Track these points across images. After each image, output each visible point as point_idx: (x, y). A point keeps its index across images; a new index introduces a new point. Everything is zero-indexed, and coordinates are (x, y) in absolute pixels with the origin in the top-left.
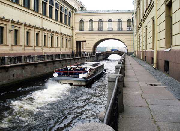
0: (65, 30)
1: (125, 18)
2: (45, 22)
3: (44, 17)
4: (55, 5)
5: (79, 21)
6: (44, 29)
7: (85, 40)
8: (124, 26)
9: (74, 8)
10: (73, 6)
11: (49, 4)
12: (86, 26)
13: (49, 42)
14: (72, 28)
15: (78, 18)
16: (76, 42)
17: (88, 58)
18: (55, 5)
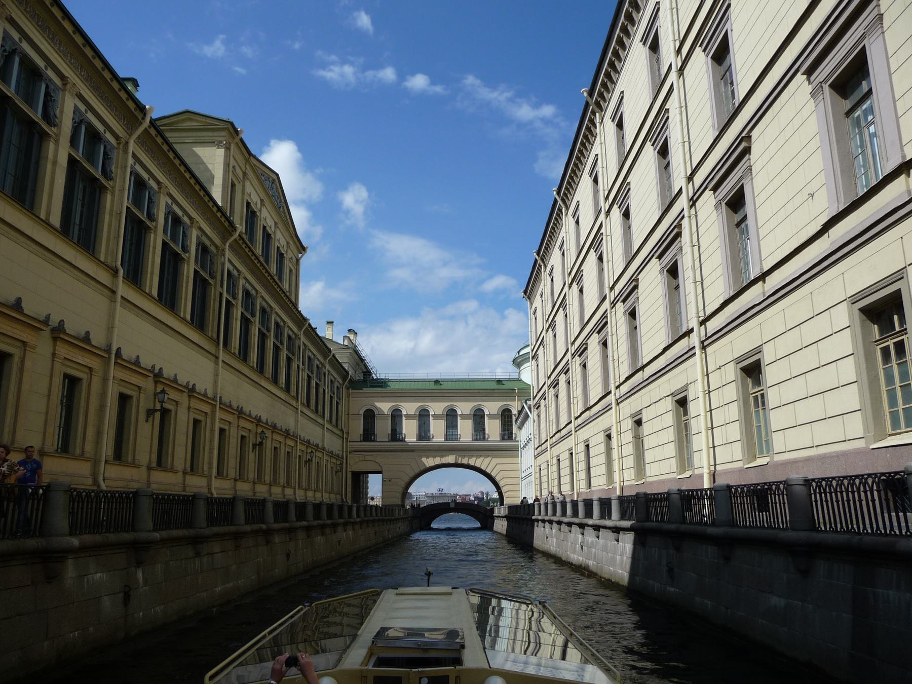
0: (310, 429)
3: (123, 289)
4: (258, 314)
5: (362, 412)
7: (379, 469)
8: (493, 428)
9: (348, 373)
10: (346, 366)
11: (192, 266)
12: (383, 428)
13: (144, 436)
14: (343, 435)
15: (359, 403)
16: (349, 475)
17: (301, 535)
18: (258, 314)
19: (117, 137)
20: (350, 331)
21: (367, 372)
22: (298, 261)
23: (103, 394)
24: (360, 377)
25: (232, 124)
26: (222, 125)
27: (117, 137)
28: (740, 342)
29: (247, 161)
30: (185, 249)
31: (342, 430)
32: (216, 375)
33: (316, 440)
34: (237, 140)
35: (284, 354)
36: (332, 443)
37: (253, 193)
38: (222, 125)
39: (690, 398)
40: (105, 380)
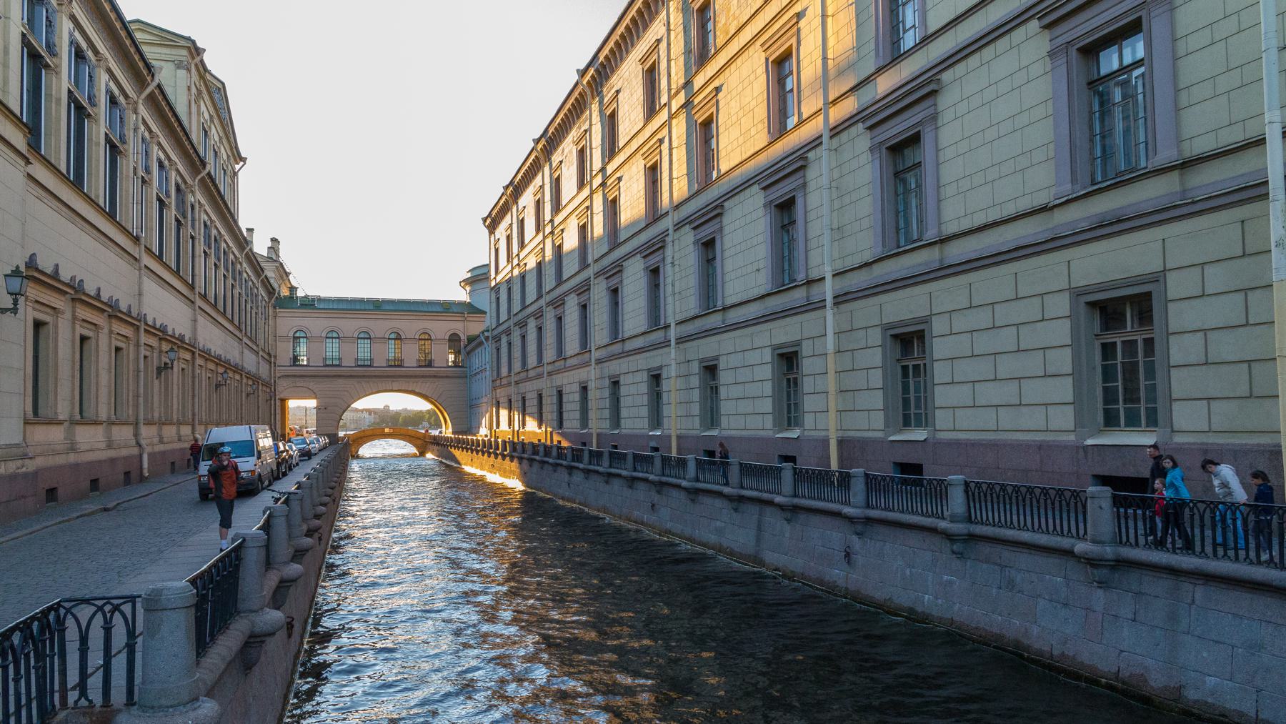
1: (441, 328)
2: (150, 285)
6: (146, 324)
19: (126, 97)
20: (274, 240)
21: (293, 289)
22: (235, 174)
23: (137, 359)
24: (285, 292)
25: (194, 42)
26: (182, 43)
27: (126, 97)
28: (706, 348)
29: (202, 77)
30: (168, 196)
31: (269, 354)
32: (195, 321)
33: (253, 370)
34: (198, 59)
35: (230, 281)
36: (264, 371)
37: (205, 109)
38: (182, 43)
39: (664, 375)
40: (137, 345)
